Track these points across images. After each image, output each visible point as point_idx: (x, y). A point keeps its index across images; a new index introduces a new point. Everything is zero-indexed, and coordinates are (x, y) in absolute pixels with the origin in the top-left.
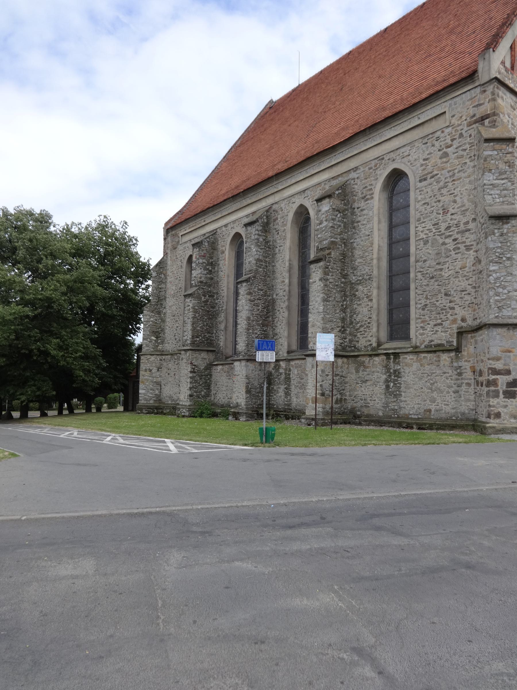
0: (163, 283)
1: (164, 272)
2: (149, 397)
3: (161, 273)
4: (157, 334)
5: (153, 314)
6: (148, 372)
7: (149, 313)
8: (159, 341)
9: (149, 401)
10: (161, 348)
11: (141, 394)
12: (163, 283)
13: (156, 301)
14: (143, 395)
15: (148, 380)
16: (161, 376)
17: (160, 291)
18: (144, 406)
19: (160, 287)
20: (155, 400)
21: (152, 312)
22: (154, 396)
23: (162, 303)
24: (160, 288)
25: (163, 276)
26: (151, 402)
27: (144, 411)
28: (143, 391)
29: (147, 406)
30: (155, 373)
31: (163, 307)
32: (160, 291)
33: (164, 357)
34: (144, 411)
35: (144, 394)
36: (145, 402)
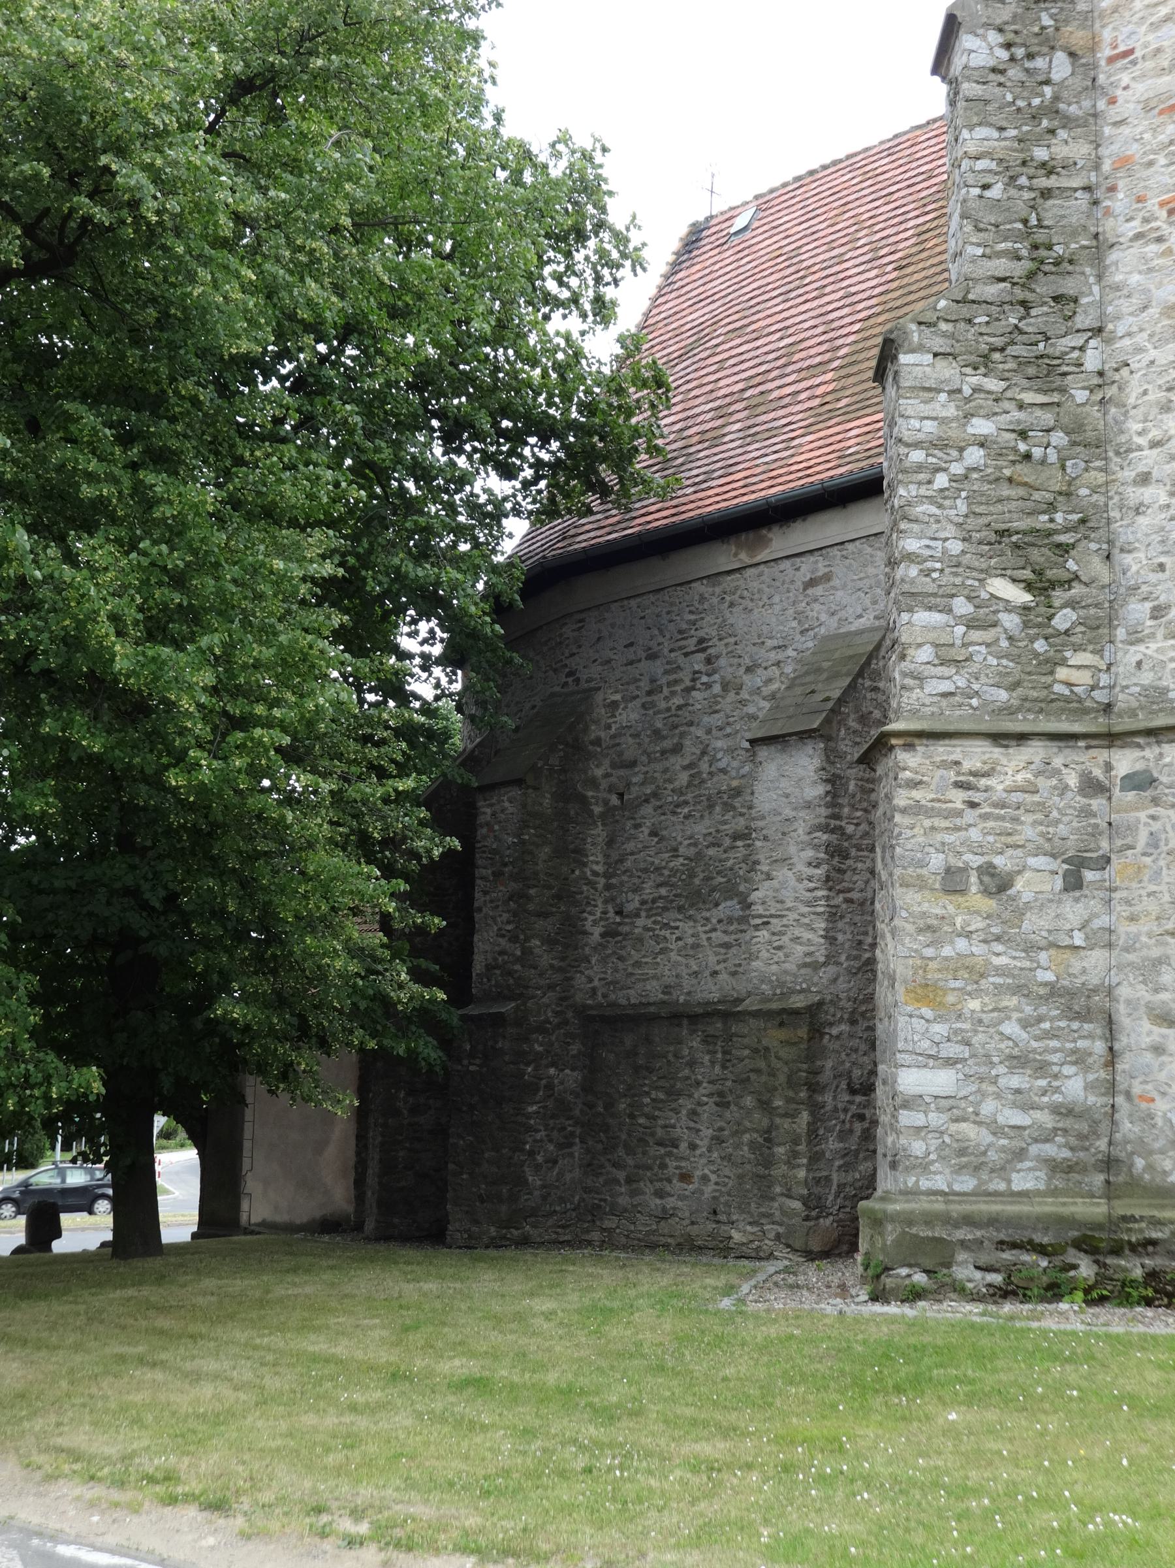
0: (1068, 122)
1: (1075, 36)
2: (997, 1130)
3: (1048, 43)
4: (1036, 555)
5: (993, 384)
6: (975, 898)
7: (947, 371)
8: (1064, 619)
9: (1002, 1170)
10: (1084, 678)
11: (910, 1103)
12: (1068, 122)
13: (1019, 269)
14: (936, 1119)
15: (977, 973)
16: (1107, 940)
17: (1046, 194)
18: (969, 1221)
19: (1041, 154)
20: (1054, 1167)
21: (983, 362)
22: (1045, 1119)
23: (1069, 286)
24: (1048, 169)
25: (1061, 69)
26: (1023, 1181)
27: (965, 1271)
28: (942, 1081)
29: (993, 1221)
30: (1041, 904)
31: (1082, 321)
32: (1046, 194)
33: (1125, 761)
34: (965, 1271)
35: (946, 1103)
36: (966, 1183)
